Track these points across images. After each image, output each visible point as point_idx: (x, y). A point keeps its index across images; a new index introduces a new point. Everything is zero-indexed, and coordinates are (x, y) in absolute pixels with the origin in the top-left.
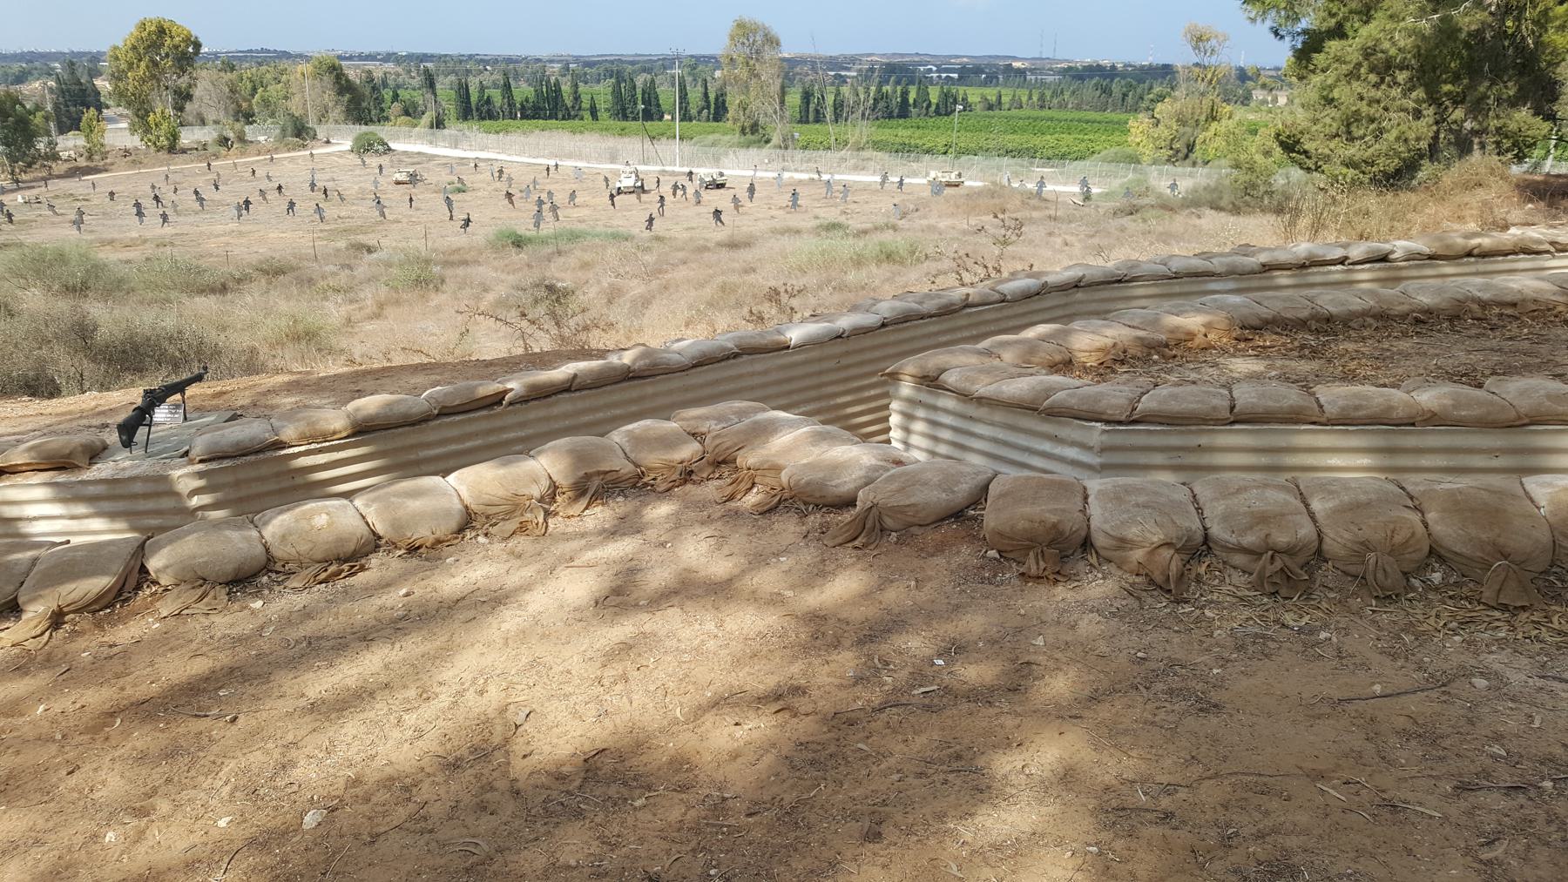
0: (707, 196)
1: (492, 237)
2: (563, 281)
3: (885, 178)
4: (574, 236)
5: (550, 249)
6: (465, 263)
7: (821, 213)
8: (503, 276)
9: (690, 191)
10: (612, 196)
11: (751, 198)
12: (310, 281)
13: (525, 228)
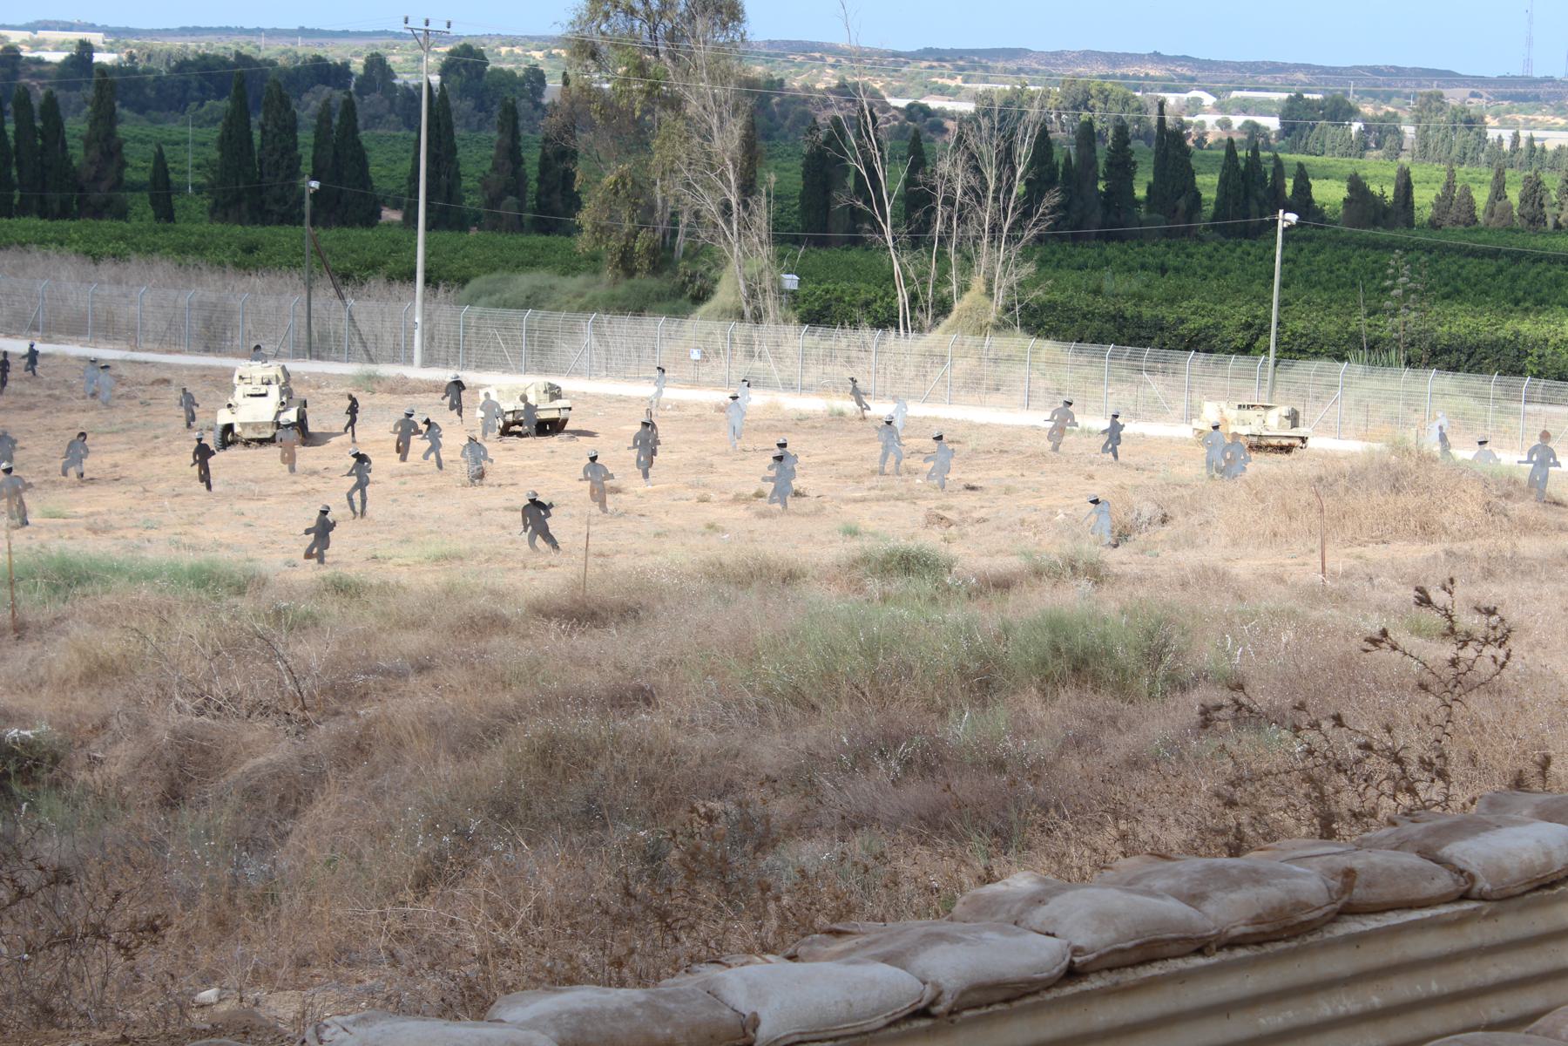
4: (69, 578)
7: (865, 517)
9: (454, 439)
10: (203, 453)
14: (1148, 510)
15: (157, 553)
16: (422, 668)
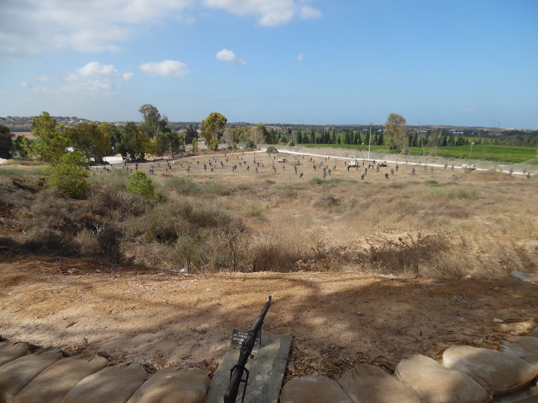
0: (382, 169)
1: (311, 180)
3: (446, 165)
4: (338, 181)
5: (330, 185)
6: (302, 189)
7: (424, 176)
9: (375, 167)
10: (348, 168)
11: (397, 170)
12: (255, 193)
13: (320, 177)
14: (459, 176)
15: (345, 178)
16: (379, 192)
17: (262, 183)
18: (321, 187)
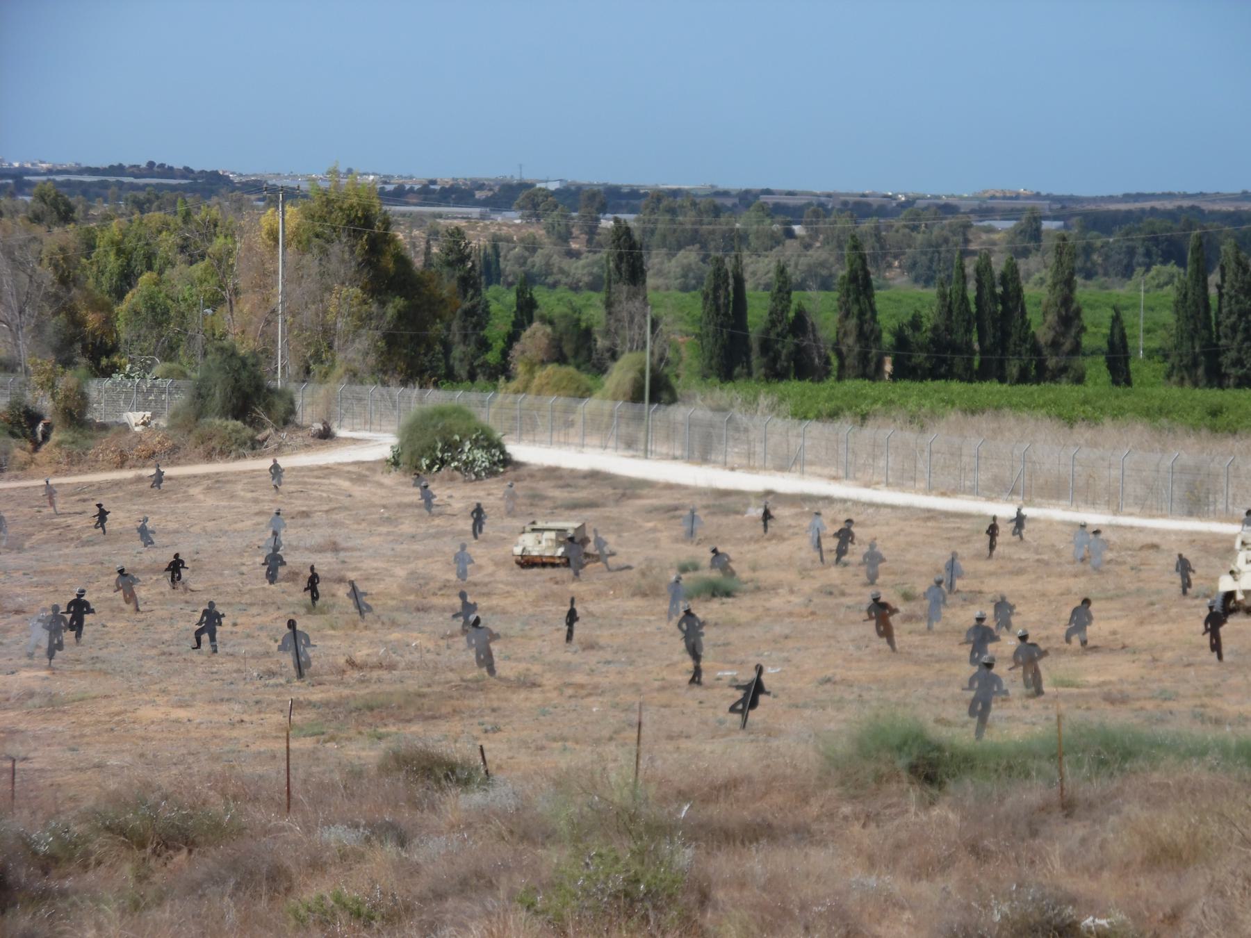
1: (843, 746)
2: (1093, 907)
4: (1115, 753)
5: (1032, 794)
8: (896, 884)
10: (1215, 621)
12: (277, 880)
15: (1182, 726)
17: (356, 774)
18: (944, 816)
